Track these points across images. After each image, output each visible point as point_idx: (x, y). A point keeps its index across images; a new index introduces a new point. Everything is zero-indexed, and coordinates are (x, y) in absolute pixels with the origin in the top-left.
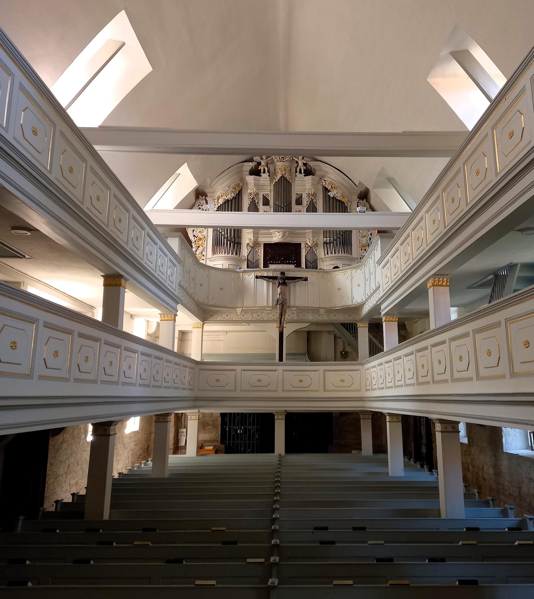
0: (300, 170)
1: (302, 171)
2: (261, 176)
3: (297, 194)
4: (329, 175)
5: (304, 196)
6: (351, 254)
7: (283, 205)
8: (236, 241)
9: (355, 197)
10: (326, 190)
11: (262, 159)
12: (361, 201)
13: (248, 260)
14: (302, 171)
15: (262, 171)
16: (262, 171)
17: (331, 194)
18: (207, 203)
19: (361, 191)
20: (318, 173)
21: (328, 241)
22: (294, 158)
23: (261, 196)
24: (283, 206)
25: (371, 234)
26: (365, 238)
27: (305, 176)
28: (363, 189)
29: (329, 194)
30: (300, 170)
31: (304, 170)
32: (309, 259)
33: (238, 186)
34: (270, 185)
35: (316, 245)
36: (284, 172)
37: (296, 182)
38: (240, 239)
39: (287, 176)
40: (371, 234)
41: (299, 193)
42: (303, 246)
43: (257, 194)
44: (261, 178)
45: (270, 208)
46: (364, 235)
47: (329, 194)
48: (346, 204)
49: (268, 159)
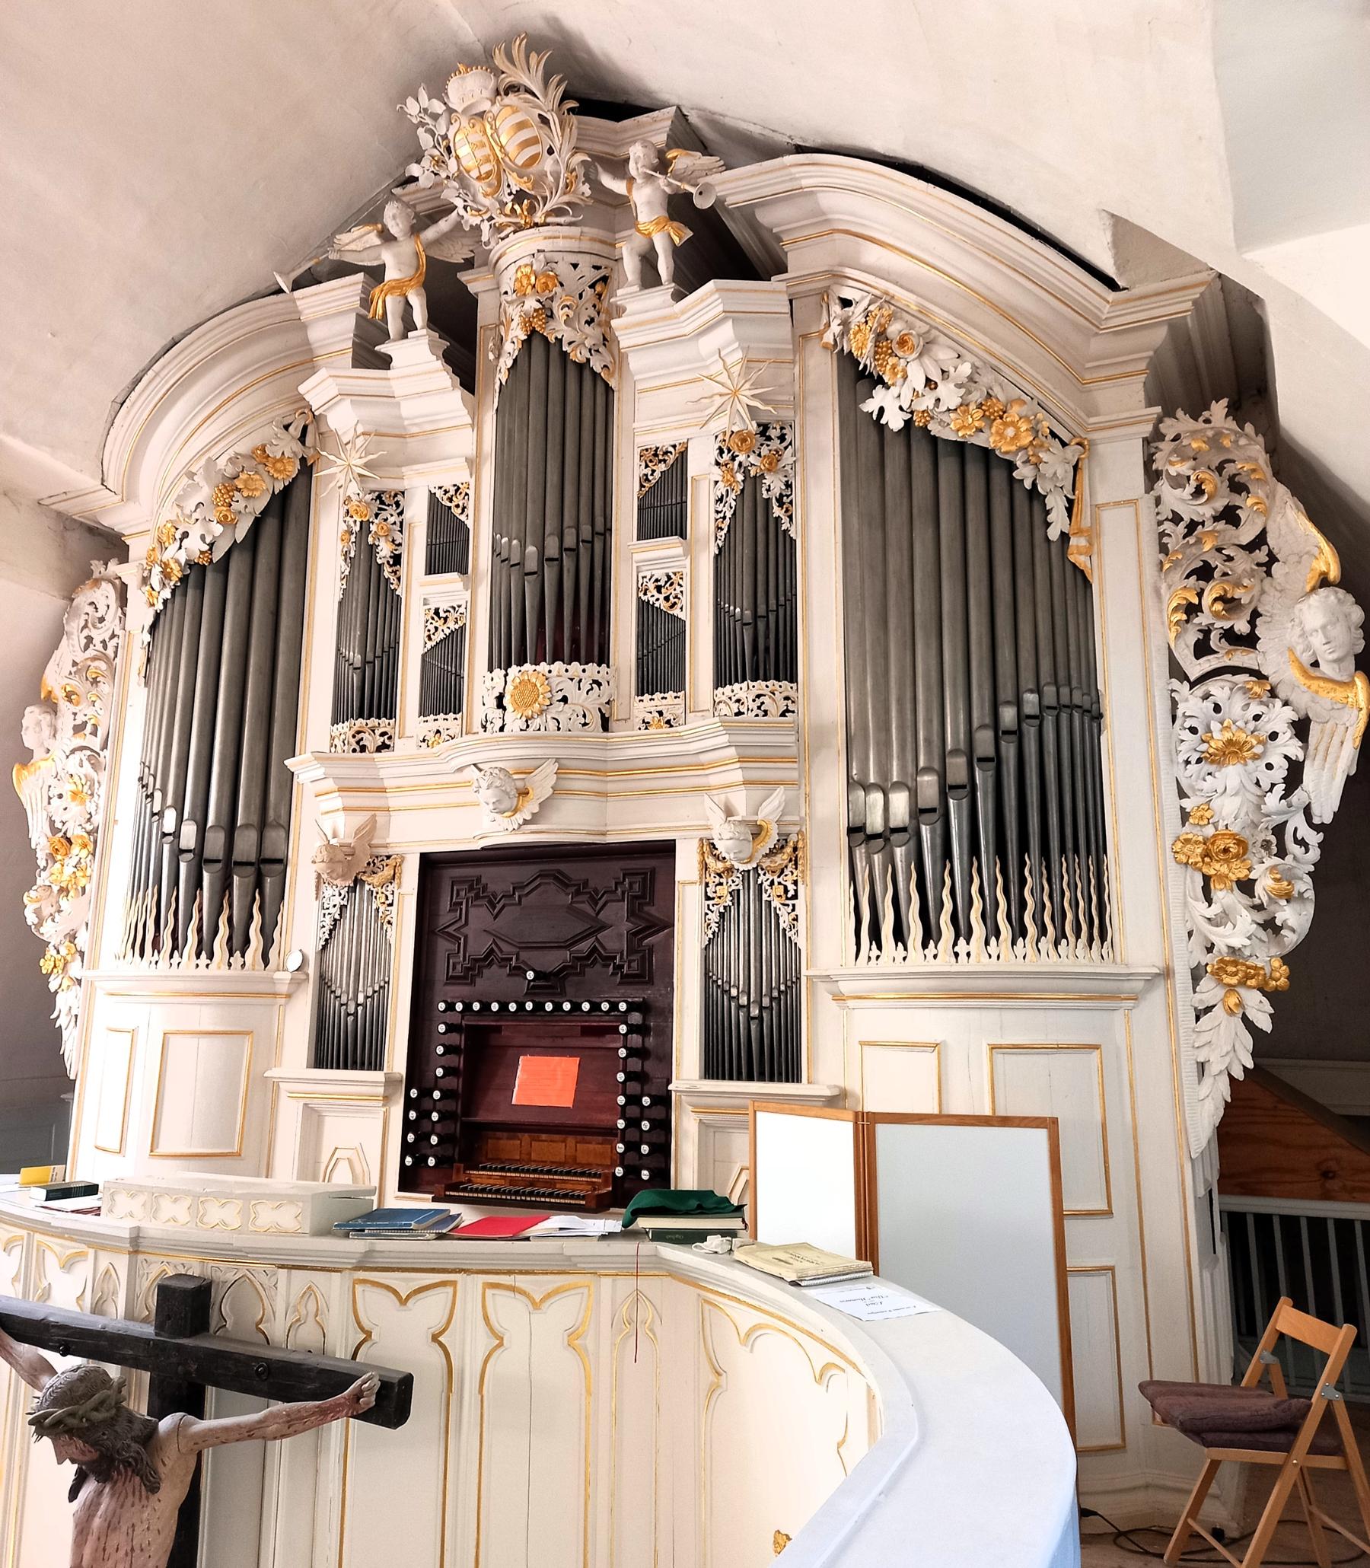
0: (648, 260)
1: (664, 267)
2: (385, 362)
3: (655, 455)
4: (872, 255)
5: (701, 464)
6: (1099, 930)
7: (531, 549)
8: (246, 845)
9: (1126, 402)
10: (859, 378)
11: (387, 237)
12: (1182, 423)
13: (324, 983)
14: (664, 267)
15: (393, 326)
16: (393, 326)
17: (889, 405)
18: (123, 601)
19: (1176, 328)
20: (802, 261)
21: (875, 823)
22: (608, 181)
23: (417, 512)
24: (532, 565)
25: (1301, 728)
26: (1232, 774)
27: (678, 296)
28: (1181, 306)
29: (870, 406)
30: (648, 260)
31: (677, 252)
32: (735, 971)
33: (261, 456)
34: (477, 424)
35: (788, 849)
36: (531, 304)
37: (634, 362)
38: (273, 835)
39: (558, 329)
40: (1301, 728)
41: (663, 440)
42: (686, 865)
43: (388, 501)
44: (395, 380)
45: (471, 586)
46: (1219, 737)
47: (870, 406)
48: (1024, 473)
49: (430, 233)
